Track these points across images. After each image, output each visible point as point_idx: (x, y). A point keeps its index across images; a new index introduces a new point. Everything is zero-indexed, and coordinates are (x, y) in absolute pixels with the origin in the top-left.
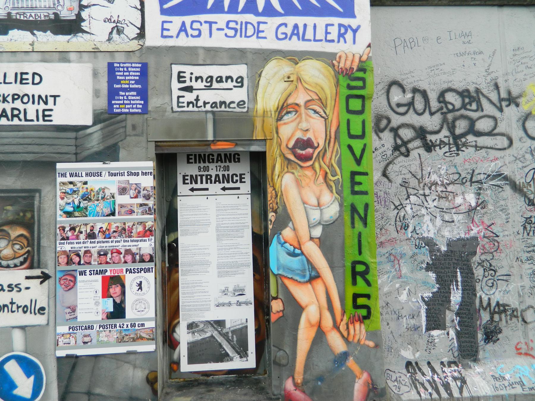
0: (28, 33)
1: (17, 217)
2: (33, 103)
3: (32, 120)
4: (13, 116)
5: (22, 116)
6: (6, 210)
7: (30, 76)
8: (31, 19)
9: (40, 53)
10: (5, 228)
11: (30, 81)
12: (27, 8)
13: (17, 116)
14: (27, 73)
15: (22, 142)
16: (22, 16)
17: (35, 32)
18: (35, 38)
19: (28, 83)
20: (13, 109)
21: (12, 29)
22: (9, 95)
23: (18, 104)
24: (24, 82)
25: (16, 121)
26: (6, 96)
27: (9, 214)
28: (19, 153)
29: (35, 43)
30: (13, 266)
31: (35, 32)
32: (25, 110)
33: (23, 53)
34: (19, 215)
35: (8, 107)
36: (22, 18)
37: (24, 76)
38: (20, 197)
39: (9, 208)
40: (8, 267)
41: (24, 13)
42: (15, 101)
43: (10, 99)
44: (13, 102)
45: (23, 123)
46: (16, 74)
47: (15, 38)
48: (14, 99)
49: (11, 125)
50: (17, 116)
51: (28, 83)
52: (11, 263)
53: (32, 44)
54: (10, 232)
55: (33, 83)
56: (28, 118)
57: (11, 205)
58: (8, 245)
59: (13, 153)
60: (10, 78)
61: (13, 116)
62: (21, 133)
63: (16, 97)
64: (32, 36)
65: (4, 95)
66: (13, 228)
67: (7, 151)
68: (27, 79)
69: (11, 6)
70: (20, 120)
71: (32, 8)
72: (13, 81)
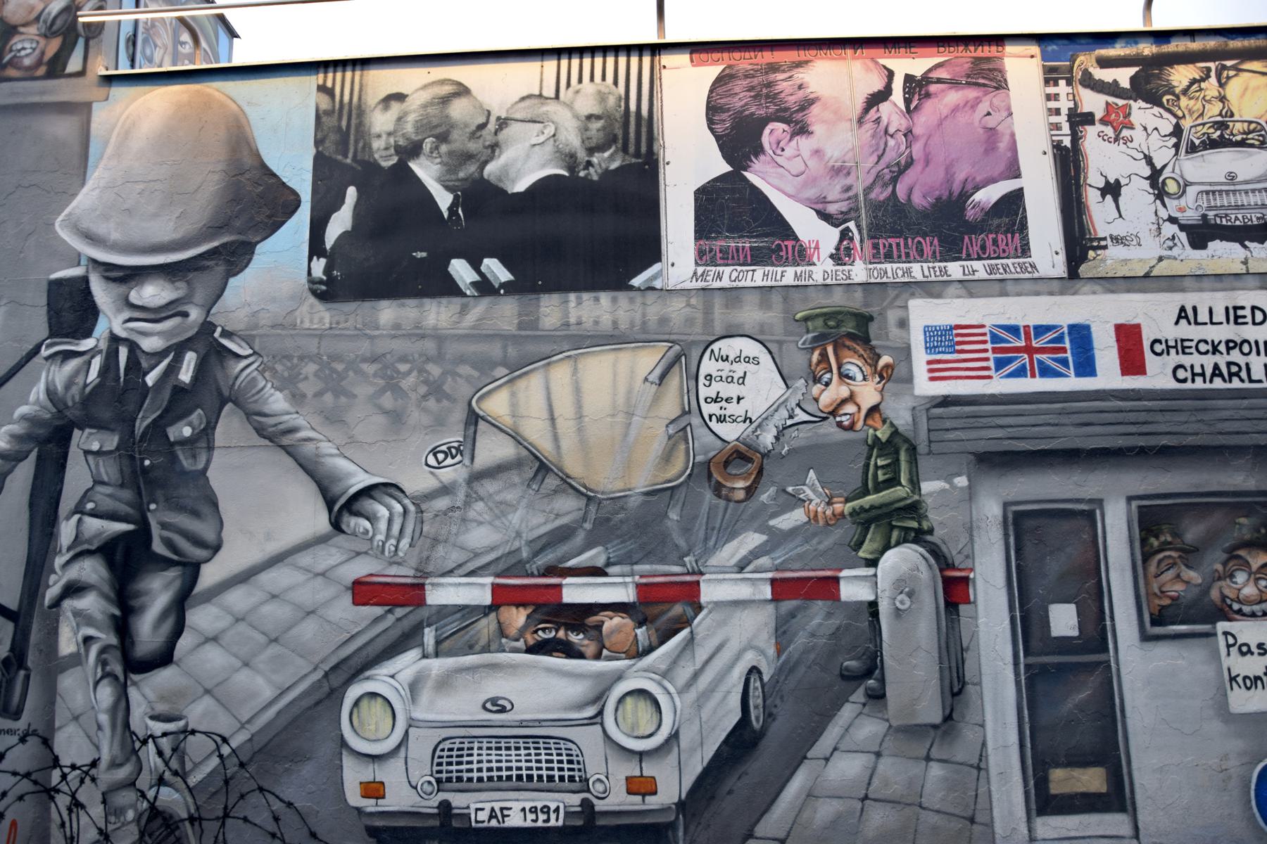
0: (1237, 245)
1: (1256, 535)
2: (1258, 353)
3: (1260, 381)
4: (1231, 375)
5: (1244, 374)
6: (1239, 524)
7: (1247, 312)
8: (1238, 223)
9: (1257, 276)
10: (1242, 553)
11: (1249, 319)
12: (1230, 207)
13: (1237, 374)
14: (1243, 308)
15: (1250, 417)
16: (1224, 220)
17: (1247, 243)
18: (1248, 253)
19: (1246, 323)
20: (1229, 364)
21: (1213, 239)
22: (1220, 342)
23: (1235, 356)
24: (1240, 320)
25: (1236, 384)
26: (1216, 343)
27: (1245, 531)
28: (1247, 433)
29: (1250, 261)
30: (1260, 614)
31: (1247, 243)
32: (1247, 365)
33: (1232, 277)
34: (1259, 531)
35: (1222, 360)
36: (1224, 222)
37: (1240, 313)
38: (1256, 503)
39: (1242, 520)
40: (1253, 615)
41: (1227, 215)
42: (1231, 352)
43: (1222, 348)
44: (1228, 353)
45: (1247, 385)
46: (1227, 309)
47: (1218, 253)
48: (1229, 349)
49: (1229, 389)
50: (1237, 374)
51: (1246, 323)
52: (1256, 608)
53: (1245, 262)
54: (1250, 560)
55: (1254, 323)
56: (1254, 377)
57: (1246, 516)
58: (1248, 580)
59: (1238, 433)
60: (1219, 316)
61: (1231, 375)
62: (1246, 402)
63: (1231, 345)
64: (1243, 250)
65: (1213, 341)
66: (1253, 553)
67: (1231, 430)
68: (1244, 317)
69: (1205, 205)
70: (1242, 381)
71: (1237, 207)
72: (1223, 319)
